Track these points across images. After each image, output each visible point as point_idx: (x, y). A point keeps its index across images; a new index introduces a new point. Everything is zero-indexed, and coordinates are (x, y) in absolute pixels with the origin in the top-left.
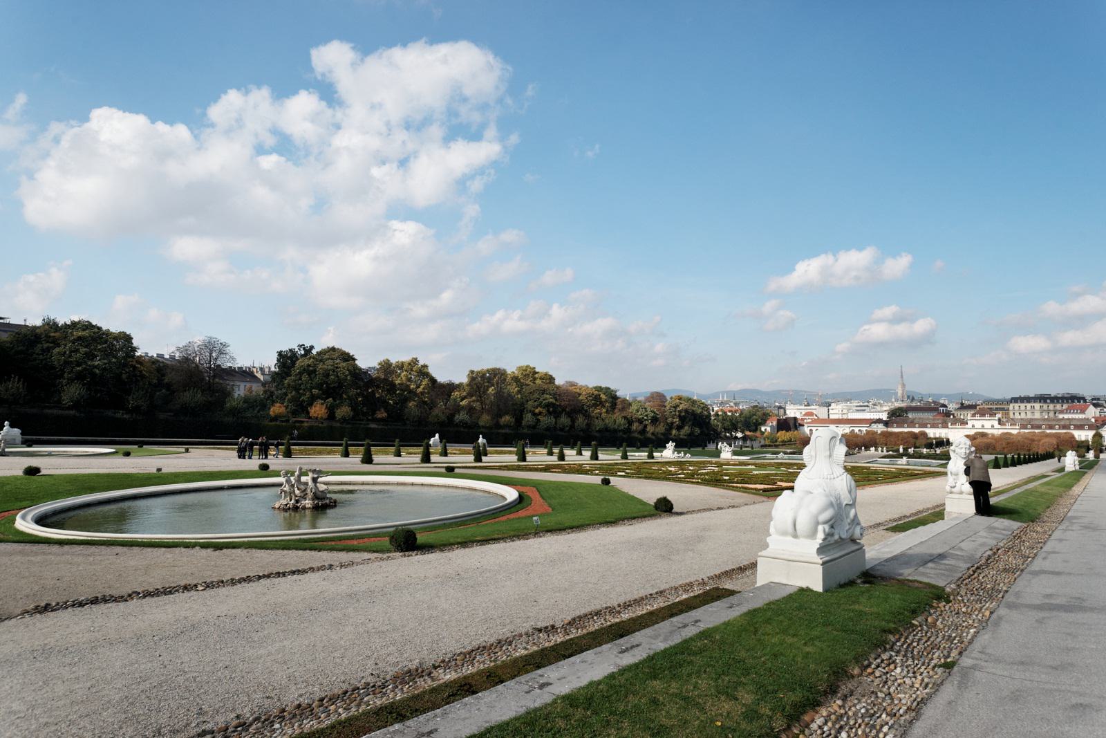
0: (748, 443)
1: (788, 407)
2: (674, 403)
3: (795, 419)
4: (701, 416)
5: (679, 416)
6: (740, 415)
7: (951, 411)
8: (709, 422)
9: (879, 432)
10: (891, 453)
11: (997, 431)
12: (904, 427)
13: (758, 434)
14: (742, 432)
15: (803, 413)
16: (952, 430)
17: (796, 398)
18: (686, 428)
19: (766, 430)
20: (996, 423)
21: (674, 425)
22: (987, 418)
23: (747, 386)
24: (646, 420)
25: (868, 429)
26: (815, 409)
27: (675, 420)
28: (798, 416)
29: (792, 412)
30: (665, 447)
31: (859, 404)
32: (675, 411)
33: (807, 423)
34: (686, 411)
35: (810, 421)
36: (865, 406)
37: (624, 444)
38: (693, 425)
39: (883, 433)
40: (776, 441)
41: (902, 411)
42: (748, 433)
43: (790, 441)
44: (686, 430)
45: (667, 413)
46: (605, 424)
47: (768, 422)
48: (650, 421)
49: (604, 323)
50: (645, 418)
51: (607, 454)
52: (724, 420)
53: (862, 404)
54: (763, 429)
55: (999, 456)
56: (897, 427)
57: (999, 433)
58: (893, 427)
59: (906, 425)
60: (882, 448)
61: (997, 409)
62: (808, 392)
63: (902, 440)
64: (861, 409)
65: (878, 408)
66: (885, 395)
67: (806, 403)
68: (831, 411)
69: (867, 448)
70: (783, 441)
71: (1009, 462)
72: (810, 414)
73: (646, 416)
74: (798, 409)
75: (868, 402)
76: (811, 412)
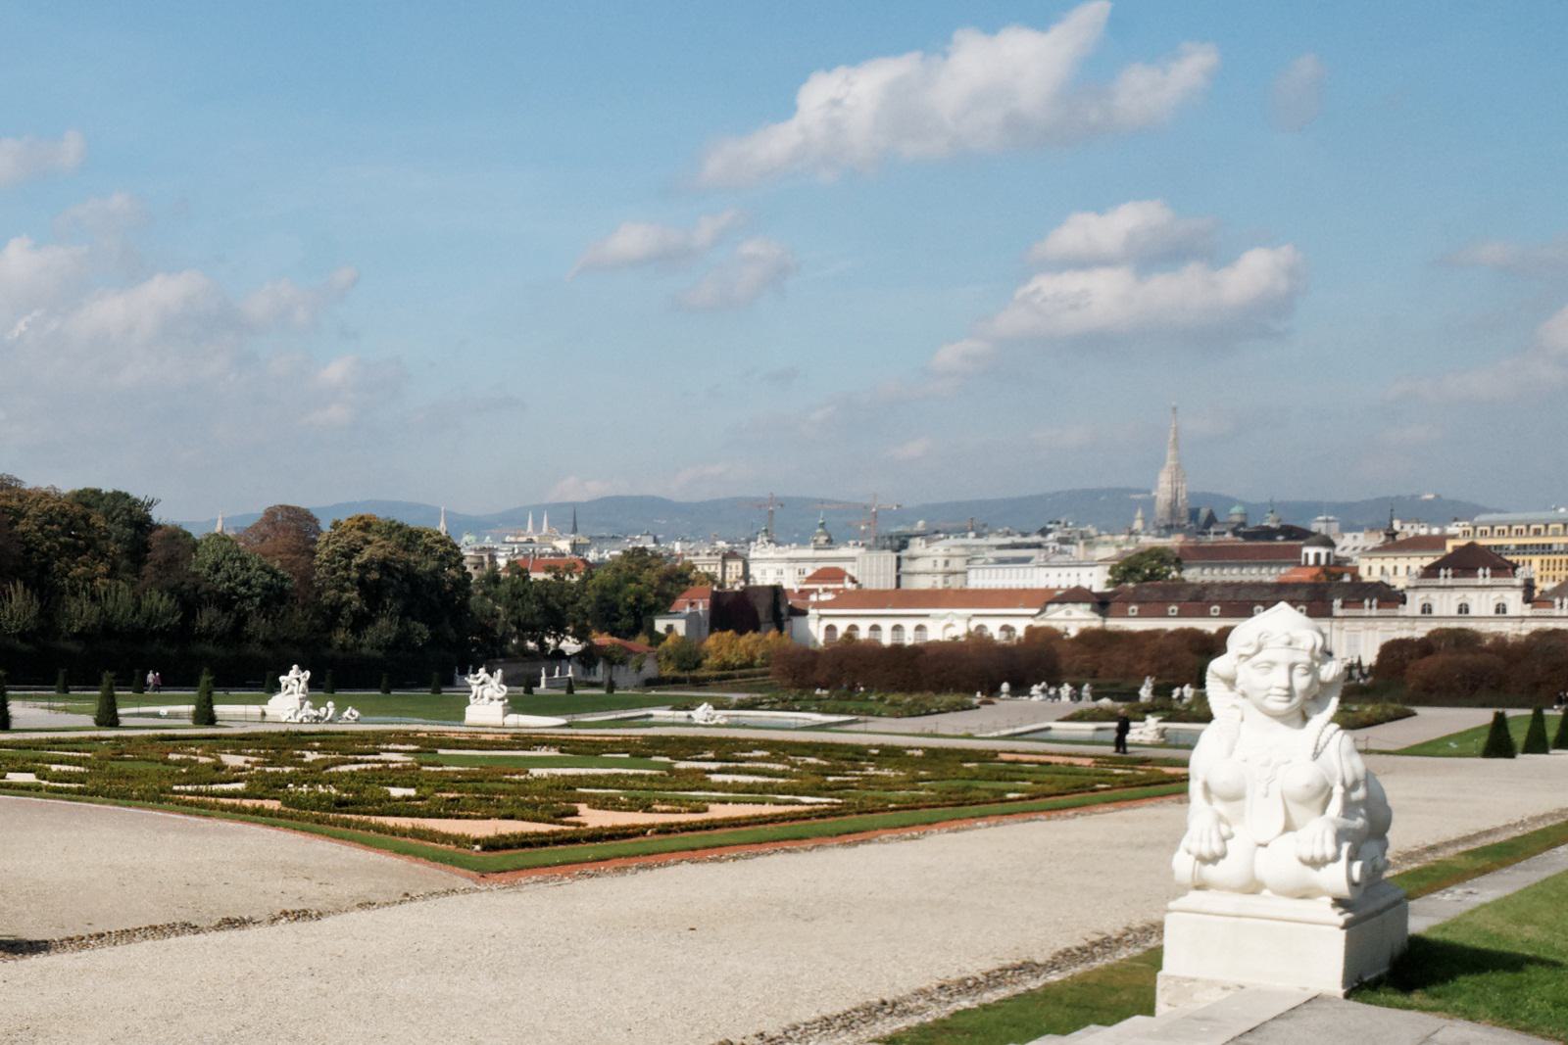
0: (600, 672)
1: (755, 552)
2: (343, 541)
3: (777, 592)
4: (435, 580)
5: (361, 583)
6: (584, 581)
7: (1348, 560)
8: (464, 605)
9: (1073, 633)
10: (1105, 702)
11: (1517, 625)
12: (1165, 615)
13: (641, 641)
14: (581, 635)
15: (810, 572)
16: (1347, 623)
17: (779, 520)
18: (383, 622)
19: (670, 628)
20: (1514, 601)
21: (345, 611)
22: (1480, 581)
23: (621, 487)
24: (243, 598)
25: (1037, 623)
26: (852, 559)
27: (346, 596)
28: (790, 582)
29: (772, 567)
30: (275, 688)
31: (1008, 540)
32: (347, 568)
33: (819, 605)
34: (385, 566)
35: (829, 597)
36: (1029, 546)
37: (107, 676)
38: (405, 613)
39: (1087, 637)
40: (698, 665)
41: (1164, 561)
42: (602, 639)
43: (750, 665)
44: (384, 628)
45: (321, 573)
46: (104, 612)
47: (680, 601)
48: (257, 600)
49: (164, 291)
50: (242, 590)
51: (66, 710)
52: (516, 596)
53: (1018, 539)
54: (660, 625)
55: (1510, 713)
56: (1141, 615)
57: (1525, 633)
58: (1125, 615)
59: (1174, 608)
60: (1077, 687)
61: (1522, 549)
62: (830, 502)
63: (1153, 660)
64: (1017, 554)
65: (1077, 551)
66: (1099, 508)
67: (822, 539)
68: (906, 566)
69: (1020, 688)
70: (725, 666)
71: (1551, 734)
72: (833, 575)
73: (246, 583)
74: (790, 560)
75: (1044, 532)
76: (836, 570)
